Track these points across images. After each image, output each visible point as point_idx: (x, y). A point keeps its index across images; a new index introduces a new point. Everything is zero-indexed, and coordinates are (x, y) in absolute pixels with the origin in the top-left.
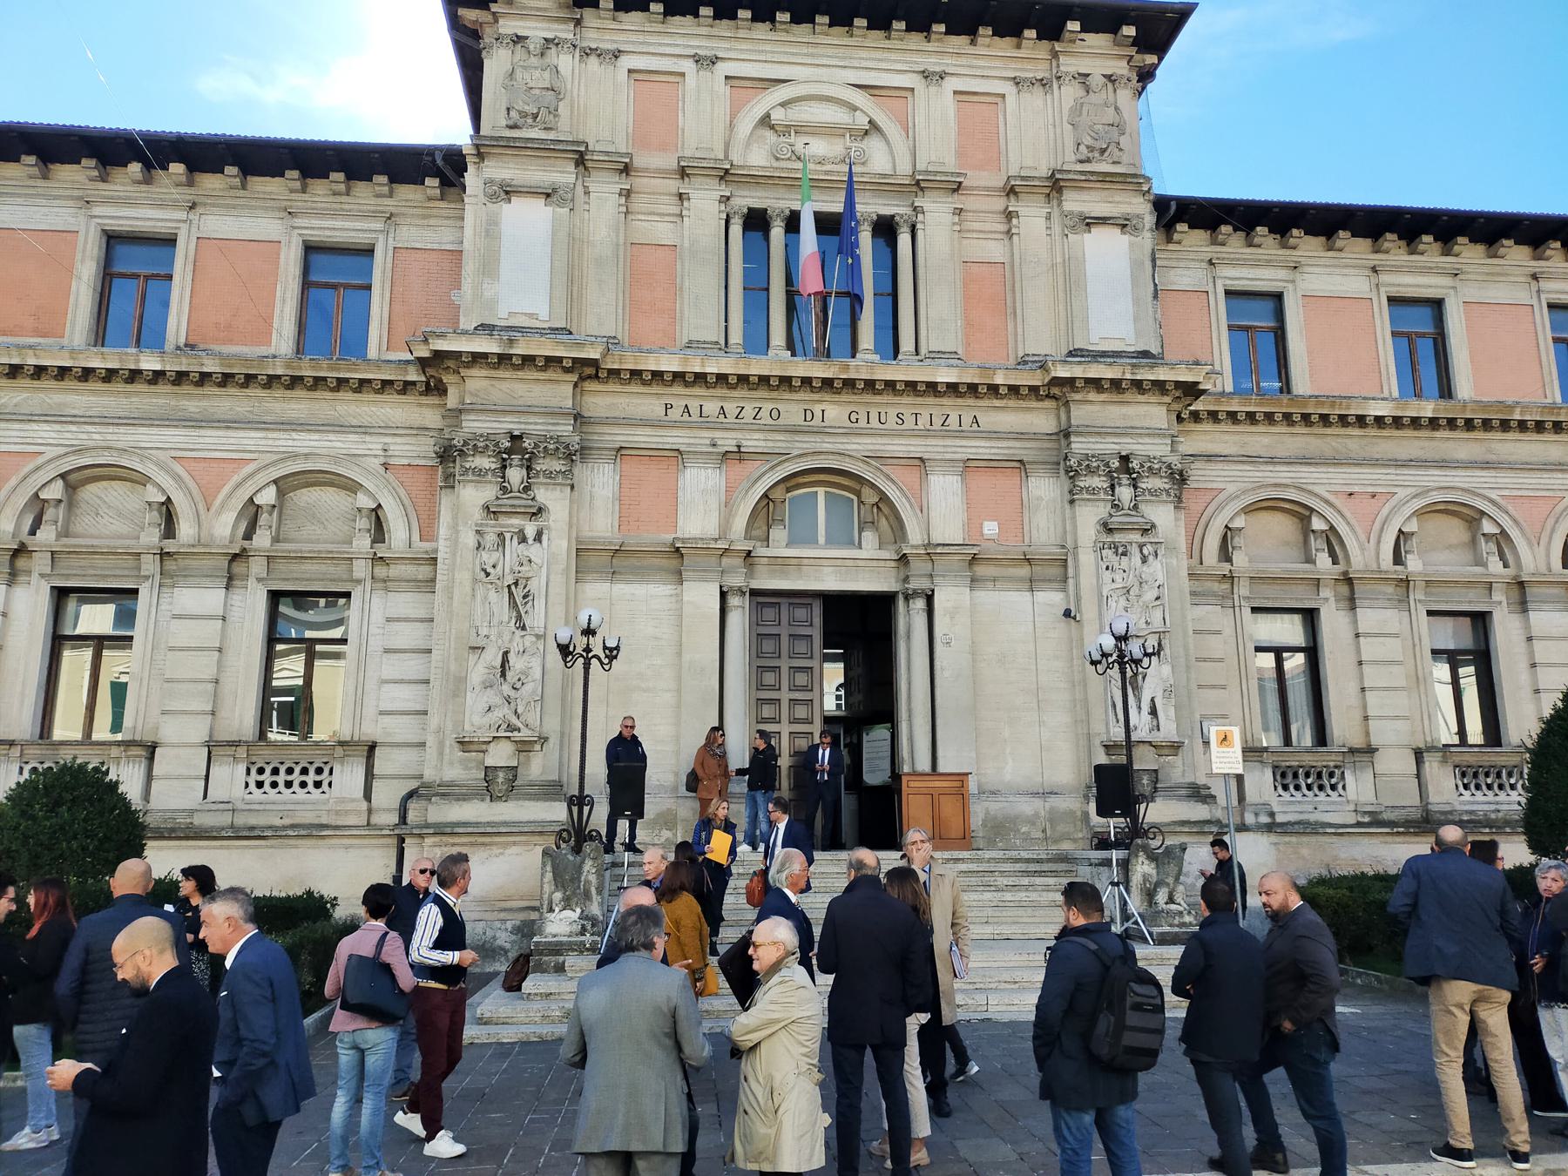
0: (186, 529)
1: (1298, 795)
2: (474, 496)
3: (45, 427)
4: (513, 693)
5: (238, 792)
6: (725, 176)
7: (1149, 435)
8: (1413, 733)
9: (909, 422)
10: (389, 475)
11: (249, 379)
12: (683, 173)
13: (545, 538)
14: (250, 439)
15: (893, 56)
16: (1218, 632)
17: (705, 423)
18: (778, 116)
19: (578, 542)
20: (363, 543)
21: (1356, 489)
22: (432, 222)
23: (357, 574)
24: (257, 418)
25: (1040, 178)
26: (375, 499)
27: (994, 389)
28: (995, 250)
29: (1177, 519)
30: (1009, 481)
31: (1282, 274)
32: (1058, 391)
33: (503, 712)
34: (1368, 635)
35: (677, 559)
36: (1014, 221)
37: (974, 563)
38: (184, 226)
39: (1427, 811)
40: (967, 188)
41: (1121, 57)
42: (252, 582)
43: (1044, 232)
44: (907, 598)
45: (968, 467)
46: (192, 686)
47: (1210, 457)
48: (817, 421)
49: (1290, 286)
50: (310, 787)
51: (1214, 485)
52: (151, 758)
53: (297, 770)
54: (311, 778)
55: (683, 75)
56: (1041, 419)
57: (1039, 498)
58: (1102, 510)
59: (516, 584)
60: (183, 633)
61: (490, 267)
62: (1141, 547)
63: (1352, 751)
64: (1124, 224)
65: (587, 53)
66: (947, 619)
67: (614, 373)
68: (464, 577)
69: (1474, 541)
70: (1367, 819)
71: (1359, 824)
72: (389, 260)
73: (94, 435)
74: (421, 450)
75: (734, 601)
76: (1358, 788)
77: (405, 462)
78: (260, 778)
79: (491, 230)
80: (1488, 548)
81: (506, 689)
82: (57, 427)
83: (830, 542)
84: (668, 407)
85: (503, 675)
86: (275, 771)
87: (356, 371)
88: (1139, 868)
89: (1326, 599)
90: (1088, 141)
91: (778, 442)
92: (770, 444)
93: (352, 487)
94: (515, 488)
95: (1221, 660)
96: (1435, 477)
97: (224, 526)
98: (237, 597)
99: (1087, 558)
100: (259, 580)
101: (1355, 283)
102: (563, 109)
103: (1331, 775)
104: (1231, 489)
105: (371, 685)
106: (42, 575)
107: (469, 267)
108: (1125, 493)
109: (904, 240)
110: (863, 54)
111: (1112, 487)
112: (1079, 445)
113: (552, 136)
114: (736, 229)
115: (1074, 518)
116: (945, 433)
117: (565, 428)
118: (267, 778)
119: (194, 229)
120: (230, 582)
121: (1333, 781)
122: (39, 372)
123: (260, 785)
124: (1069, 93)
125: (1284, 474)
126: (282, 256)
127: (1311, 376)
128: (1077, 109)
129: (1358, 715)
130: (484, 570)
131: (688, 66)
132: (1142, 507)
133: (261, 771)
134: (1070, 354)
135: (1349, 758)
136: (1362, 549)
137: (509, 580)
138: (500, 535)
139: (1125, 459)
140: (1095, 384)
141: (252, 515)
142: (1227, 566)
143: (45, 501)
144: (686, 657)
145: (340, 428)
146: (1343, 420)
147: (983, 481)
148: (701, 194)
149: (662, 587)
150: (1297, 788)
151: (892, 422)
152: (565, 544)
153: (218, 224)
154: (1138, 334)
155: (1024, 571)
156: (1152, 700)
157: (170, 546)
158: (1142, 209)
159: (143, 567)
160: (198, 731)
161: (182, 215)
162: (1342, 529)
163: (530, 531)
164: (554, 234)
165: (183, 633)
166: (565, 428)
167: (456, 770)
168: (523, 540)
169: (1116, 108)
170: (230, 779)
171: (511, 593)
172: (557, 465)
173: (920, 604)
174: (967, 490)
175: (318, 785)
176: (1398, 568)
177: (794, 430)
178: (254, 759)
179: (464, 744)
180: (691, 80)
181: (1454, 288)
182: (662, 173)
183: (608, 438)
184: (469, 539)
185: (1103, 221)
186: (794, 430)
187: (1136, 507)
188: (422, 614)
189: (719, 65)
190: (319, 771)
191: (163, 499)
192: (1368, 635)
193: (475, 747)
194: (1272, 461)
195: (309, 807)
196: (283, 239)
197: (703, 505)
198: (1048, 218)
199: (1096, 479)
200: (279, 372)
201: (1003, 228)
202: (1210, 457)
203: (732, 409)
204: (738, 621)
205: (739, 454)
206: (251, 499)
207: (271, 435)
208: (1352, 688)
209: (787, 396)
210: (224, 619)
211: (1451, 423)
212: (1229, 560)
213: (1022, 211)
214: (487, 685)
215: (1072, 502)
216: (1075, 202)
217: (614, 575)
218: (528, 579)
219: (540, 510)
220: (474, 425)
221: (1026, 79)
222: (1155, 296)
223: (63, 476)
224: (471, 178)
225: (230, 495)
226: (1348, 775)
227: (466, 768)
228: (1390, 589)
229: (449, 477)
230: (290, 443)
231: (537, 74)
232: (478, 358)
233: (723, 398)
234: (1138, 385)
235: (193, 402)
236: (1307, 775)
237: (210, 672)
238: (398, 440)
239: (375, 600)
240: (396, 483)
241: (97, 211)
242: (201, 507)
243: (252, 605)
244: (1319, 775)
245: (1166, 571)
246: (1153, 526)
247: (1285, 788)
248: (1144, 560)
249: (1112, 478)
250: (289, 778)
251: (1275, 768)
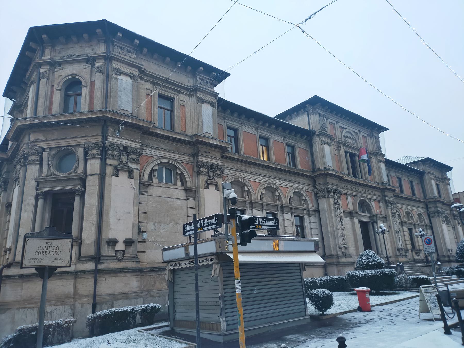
6: (344, 145)
14: (288, 183)
30: (377, 203)
33: (344, 241)
39: (414, 259)
44: (373, 224)
45: (375, 200)
61: (323, 156)
69: (408, 217)
79: (323, 149)
80: (411, 218)
99: (391, 218)
131: (335, 123)
155: (382, 219)
158: (384, 160)
161: (270, 134)
179: (339, 247)
184: (332, 208)
188: (314, 221)
205: (353, 195)
216: (380, 158)
235: (280, 176)
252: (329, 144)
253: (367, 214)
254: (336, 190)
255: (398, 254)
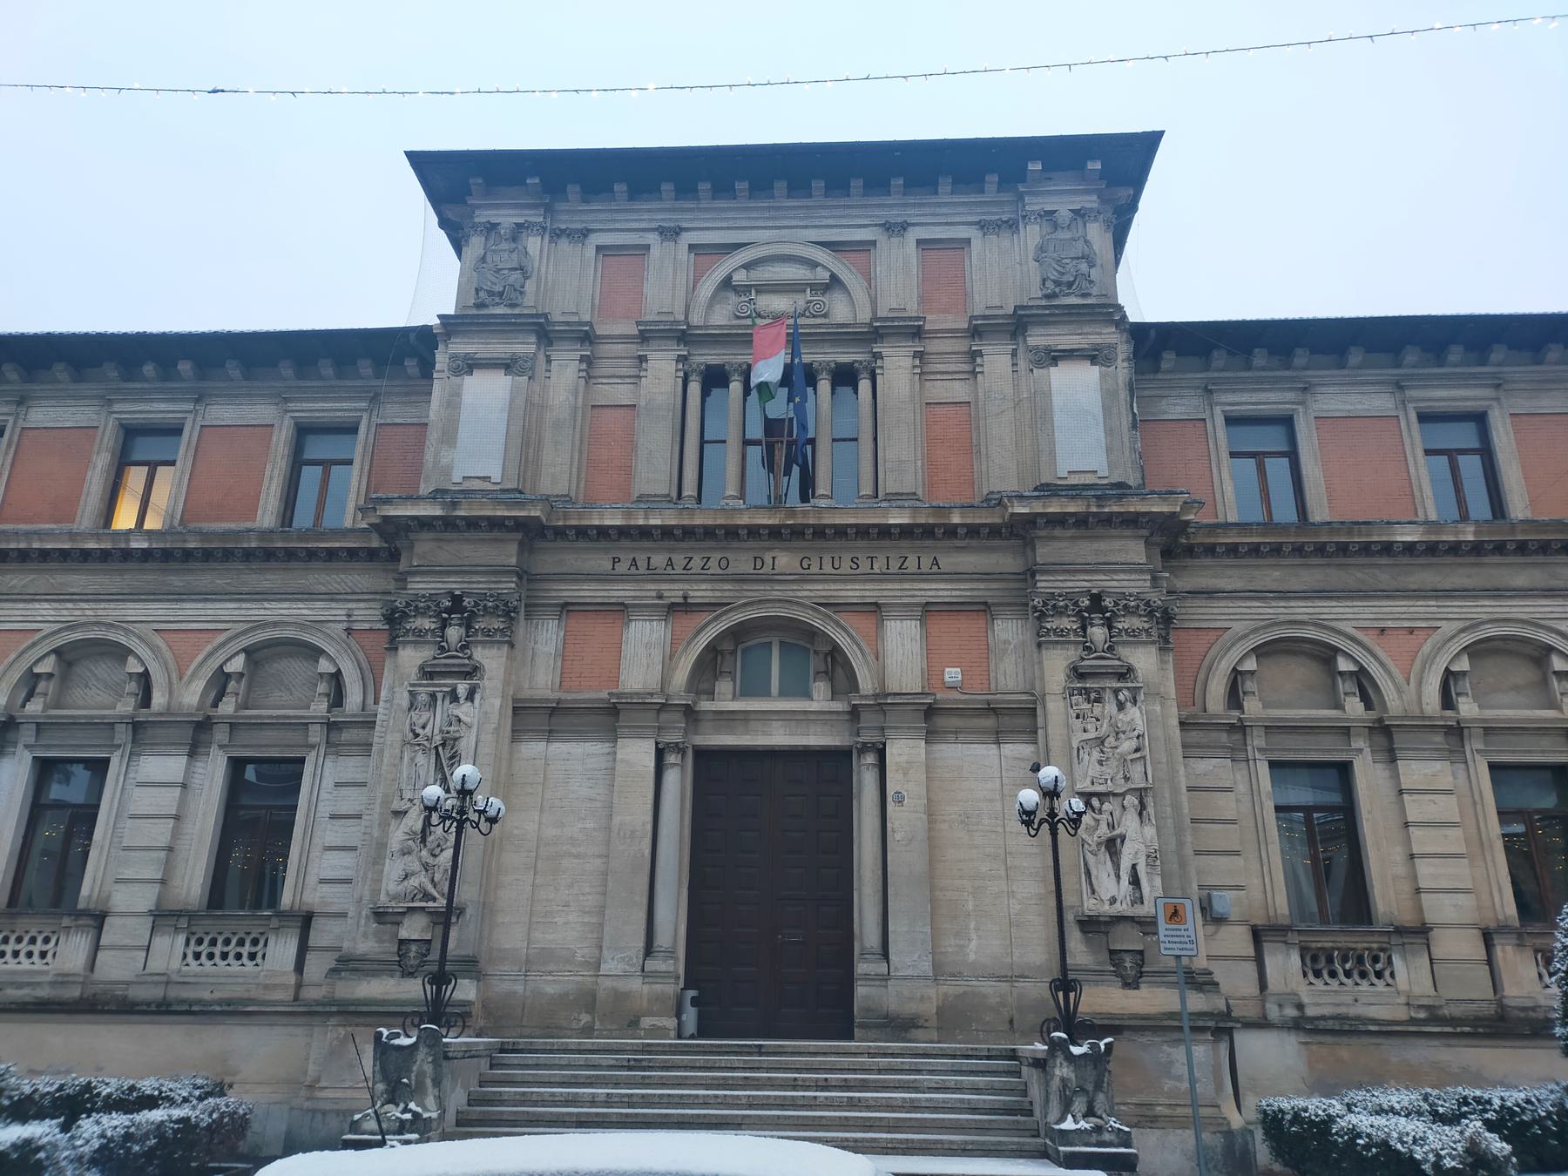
0: (159, 699)
1: (1334, 984)
2: (411, 658)
3: (46, 605)
4: (430, 860)
5: (176, 963)
7: (1124, 571)
8: (1479, 908)
9: (864, 567)
10: (352, 641)
11: (228, 555)
12: (644, 337)
13: (477, 697)
15: (854, 212)
16: (1229, 790)
17: (653, 575)
18: (740, 277)
19: (515, 700)
20: (320, 708)
21: (1390, 624)
22: (414, 398)
23: (313, 739)
24: (233, 589)
25: (1003, 316)
26: (336, 664)
27: (951, 531)
28: (958, 390)
29: (1163, 662)
30: (968, 625)
31: (1290, 396)
32: (1021, 531)
33: (420, 880)
34: (1411, 792)
35: (610, 717)
36: (979, 360)
37: (933, 717)
38: (190, 417)
39: (1500, 1004)
40: (929, 332)
41: (1087, 192)
42: (214, 750)
43: (1010, 369)
45: (928, 611)
46: (143, 853)
47: (1211, 594)
48: (767, 569)
49: (1301, 409)
50: (245, 960)
51: (1218, 624)
52: (100, 928)
53: (234, 942)
54: (245, 950)
55: (647, 247)
56: (1005, 561)
57: (1006, 642)
58: (1072, 654)
59: (443, 745)
60: (144, 800)
61: (449, 436)
62: (1116, 691)
63: (1400, 931)
64: (1094, 356)
65: (556, 235)
66: (900, 776)
67: (560, 533)
68: (393, 738)
70: (1422, 1015)
71: (1413, 1021)
72: (371, 436)
73: (87, 611)
74: (368, 614)
75: (672, 758)
76: (1410, 974)
77: (367, 626)
78: (199, 949)
79: (453, 402)
81: (424, 853)
82: (56, 605)
83: (784, 693)
84: (616, 561)
85: (424, 840)
86: (213, 943)
87: (323, 541)
88: (1057, 1072)
89: (1360, 751)
90: (1054, 275)
91: (725, 591)
92: (718, 594)
93: (316, 653)
94: (453, 647)
95: (1233, 822)
96: (1486, 608)
97: (192, 695)
98: (199, 766)
99: (1056, 710)
100: (221, 747)
101: (1379, 402)
102: (530, 286)
103: (1376, 960)
104: (1238, 627)
105: (315, 853)
106: (26, 746)
107: (433, 436)
108: (1098, 633)
109: (864, 385)
110: (824, 213)
111: (1084, 628)
112: (1045, 583)
113: (516, 311)
114: (695, 388)
115: (1041, 663)
116: (903, 576)
117: (508, 585)
118: (204, 948)
119: (199, 418)
120: (195, 750)
121: (1379, 966)
122: (45, 555)
123: (197, 956)
124: (1032, 234)
125: (1301, 609)
126: (274, 438)
127: (1330, 501)
128: (1041, 249)
129: (1406, 887)
130: (413, 731)
131: (652, 238)
132: (1123, 651)
133: (200, 942)
134: (1036, 489)
135: (1395, 940)
136: (1399, 691)
137: (438, 739)
138: (433, 696)
139: (1096, 599)
140: (1059, 520)
141: (221, 681)
142: (1236, 713)
143: (38, 675)
144: (617, 820)
145: (308, 596)
146: (1366, 549)
147: (941, 625)
148: (659, 355)
149: (600, 745)
150: (1333, 974)
151: (846, 567)
152: (497, 702)
153: (222, 413)
154: (1111, 465)
155: (989, 722)
156: (1134, 867)
157: (143, 716)
159: (117, 735)
160: (145, 899)
162: (1374, 669)
163: (462, 688)
164: (512, 401)
165: (144, 800)
166: (508, 585)
167: (366, 944)
168: (455, 698)
169: (1086, 241)
170: (169, 952)
171: (437, 754)
172: (497, 624)
173: (870, 759)
174: (926, 636)
175: (252, 956)
176: (1449, 713)
177: (741, 579)
178: (194, 929)
179: (380, 915)
180: (655, 252)
181: (1497, 399)
182: (625, 338)
183: (554, 594)
185: (1070, 355)
186: (741, 579)
187: (1111, 649)
189: (685, 235)
190: (255, 942)
191: (141, 670)
192: (1411, 792)
193: (389, 918)
194: (1284, 595)
195: (241, 980)
196: (276, 422)
197: (646, 656)
198: (1014, 354)
199: (1065, 620)
200: (253, 545)
201: (967, 367)
202: (1211, 594)
203: (680, 560)
204: (677, 782)
205: (683, 607)
206: (221, 666)
207: (244, 605)
208: (1398, 853)
209: (735, 544)
210: (184, 786)
211: (1500, 548)
212: (1240, 707)
213: (986, 349)
214: (405, 852)
215: (1039, 645)
216: (1038, 338)
217: (550, 735)
218: (456, 739)
219: (476, 669)
220: (420, 586)
221: (990, 223)
222: (1134, 426)
223: (57, 651)
224: (441, 358)
225: (201, 665)
226: (1396, 960)
227: (380, 941)
228: (1439, 738)
229: (393, 639)
230: (262, 612)
231: (506, 255)
232: (424, 523)
233: (672, 550)
234: (1108, 520)
235: (177, 581)
236: (1345, 960)
237: (163, 840)
238: (362, 605)
239: (328, 764)
240: (355, 647)
241: (117, 407)
242: (174, 676)
243: (213, 773)
244: (1360, 960)
245: (1147, 719)
246: (1130, 669)
247: (1318, 974)
248: (1121, 706)
249: (1083, 618)
250: (226, 949)
251: (1304, 951)
252: (508, 365)
253: (820, 699)
254: (457, 600)
255: (1080, 952)
